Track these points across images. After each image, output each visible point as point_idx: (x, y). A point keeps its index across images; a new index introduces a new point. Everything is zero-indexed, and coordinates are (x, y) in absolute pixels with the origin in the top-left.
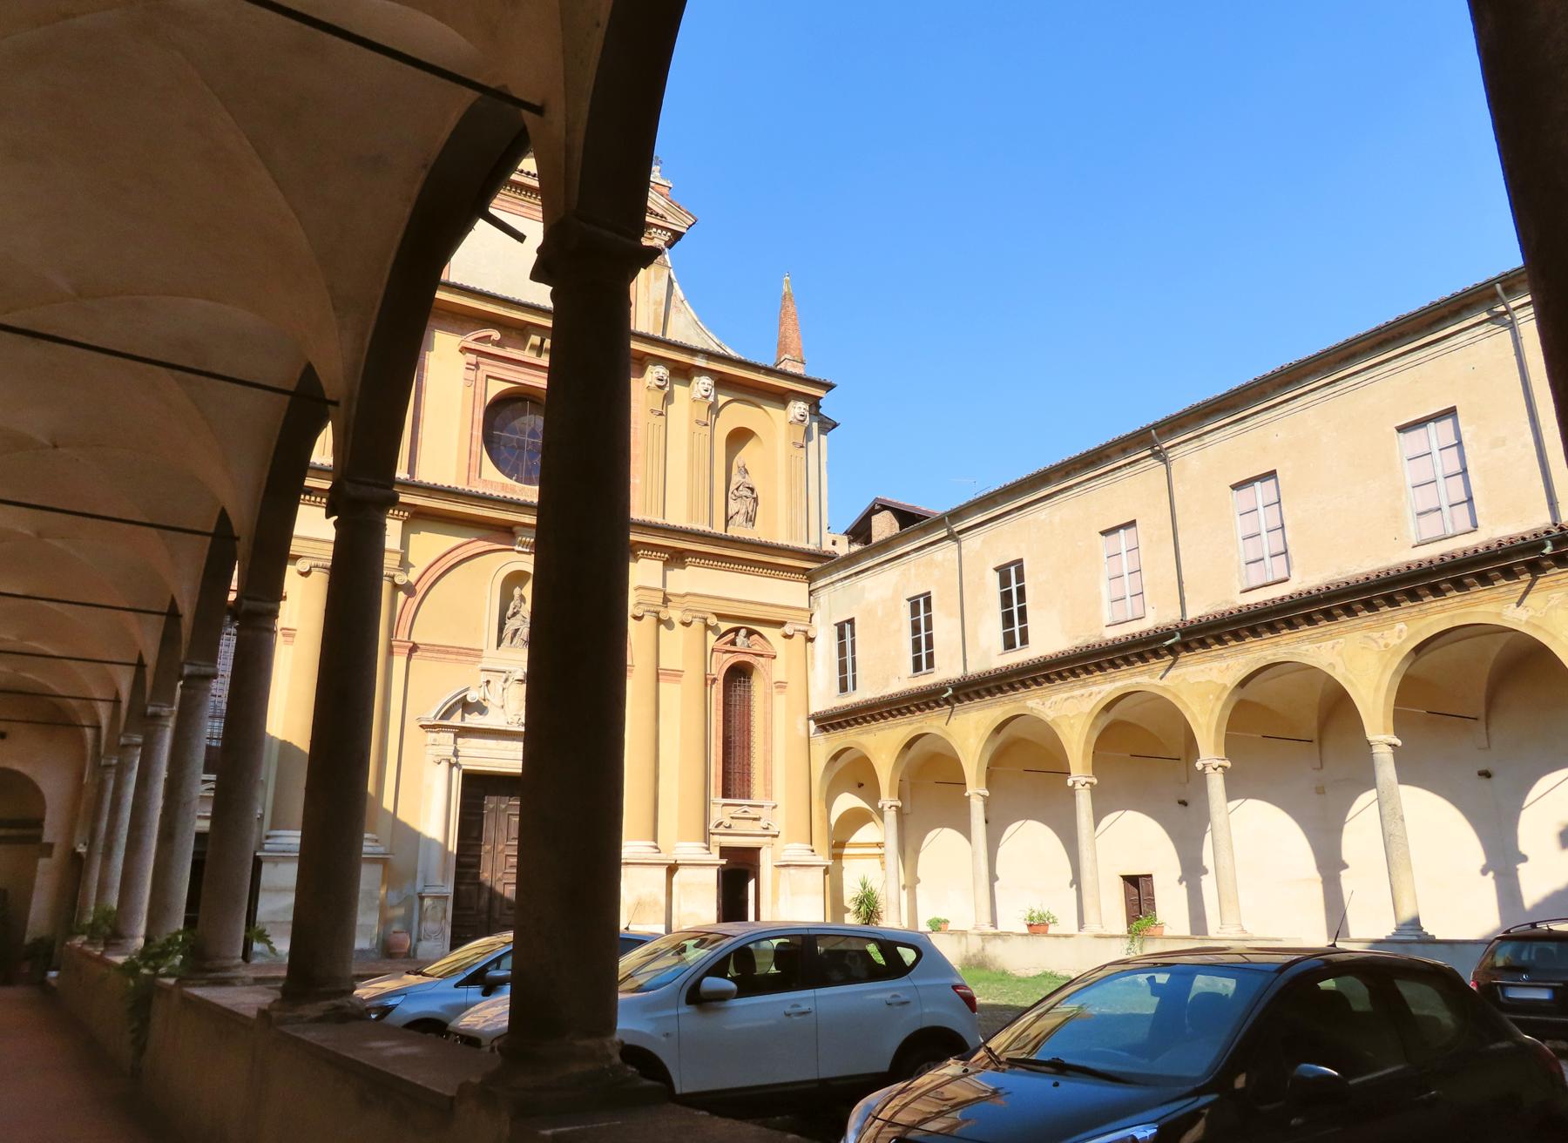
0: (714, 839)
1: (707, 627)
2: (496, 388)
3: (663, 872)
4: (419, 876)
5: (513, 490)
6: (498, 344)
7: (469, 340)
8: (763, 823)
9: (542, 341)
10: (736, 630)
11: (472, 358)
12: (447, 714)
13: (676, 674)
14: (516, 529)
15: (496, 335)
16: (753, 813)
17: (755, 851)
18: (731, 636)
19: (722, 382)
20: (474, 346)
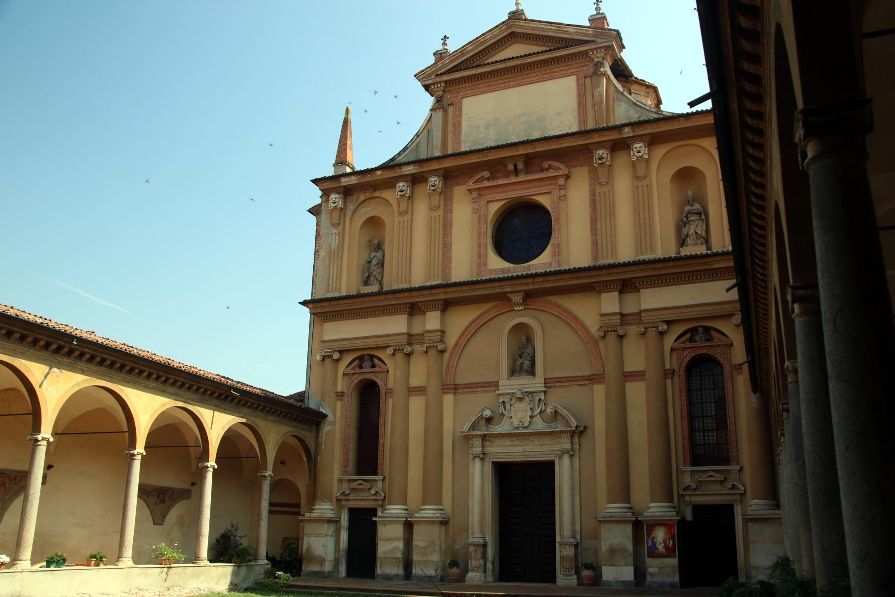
0: (687, 499)
1: (662, 334)
2: (494, 208)
3: (629, 529)
4: (470, 531)
5: (508, 270)
6: (488, 179)
7: (471, 184)
8: (729, 485)
9: (515, 166)
10: (694, 331)
11: (475, 195)
12: (474, 427)
13: (638, 376)
14: (509, 295)
15: (486, 174)
16: (719, 477)
17: (727, 510)
18: (689, 335)
19: (653, 141)
20: (473, 187)
